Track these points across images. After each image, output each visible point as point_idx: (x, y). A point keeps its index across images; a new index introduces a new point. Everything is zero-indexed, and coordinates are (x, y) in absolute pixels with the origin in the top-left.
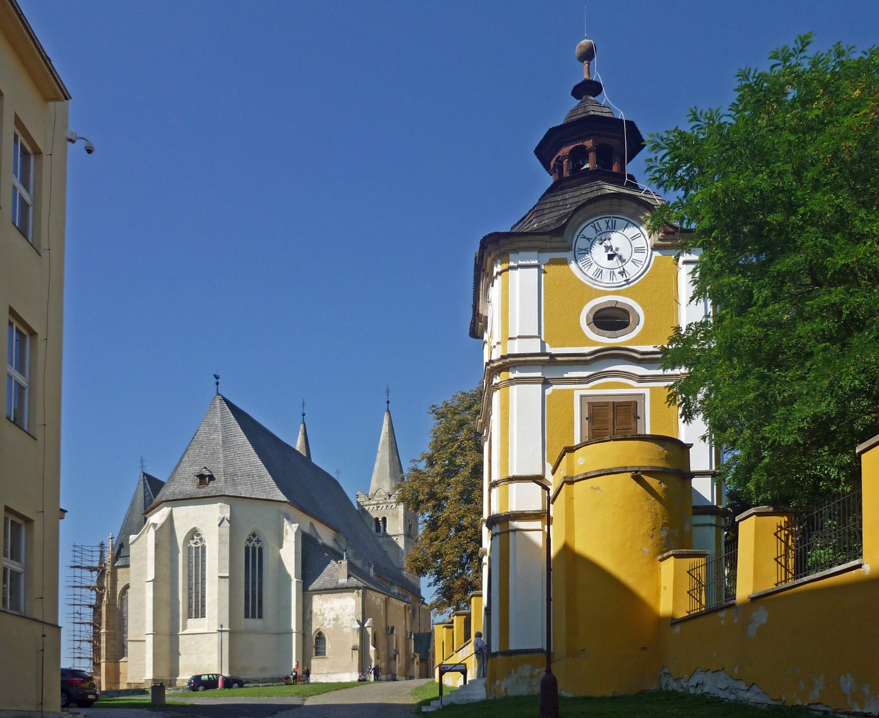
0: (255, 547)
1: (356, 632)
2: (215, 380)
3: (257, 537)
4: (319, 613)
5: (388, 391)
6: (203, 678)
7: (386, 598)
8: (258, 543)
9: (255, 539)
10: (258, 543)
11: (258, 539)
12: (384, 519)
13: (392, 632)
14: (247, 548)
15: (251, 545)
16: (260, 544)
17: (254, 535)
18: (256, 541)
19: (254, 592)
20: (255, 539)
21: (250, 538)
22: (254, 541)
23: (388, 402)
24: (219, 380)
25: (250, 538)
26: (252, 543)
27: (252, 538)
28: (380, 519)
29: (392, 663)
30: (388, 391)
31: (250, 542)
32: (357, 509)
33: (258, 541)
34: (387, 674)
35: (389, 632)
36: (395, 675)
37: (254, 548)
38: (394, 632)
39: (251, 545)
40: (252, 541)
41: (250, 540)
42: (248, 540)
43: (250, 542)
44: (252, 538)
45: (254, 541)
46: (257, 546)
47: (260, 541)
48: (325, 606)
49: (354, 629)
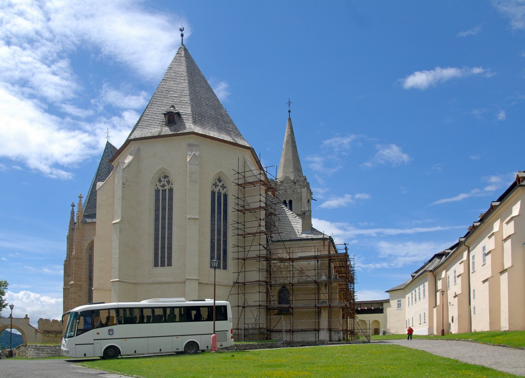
0: (221, 193)
3: (222, 183)
5: (289, 103)
8: (223, 189)
9: (220, 184)
10: (223, 189)
11: (223, 185)
14: (213, 193)
15: (216, 190)
16: (225, 190)
19: (219, 240)
20: (220, 184)
21: (216, 183)
23: (289, 111)
25: (216, 183)
26: (218, 188)
27: (218, 183)
30: (289, 103)
31: (216, 188)
33: (223, 187)
37: (219, 193)
39: (216, 190)
41: (215, 185)
42: (214, 185)
43: (216, 188)
44: (218, 183)
45: (219, 187)
46: (223, 192)
47: (225, 187)
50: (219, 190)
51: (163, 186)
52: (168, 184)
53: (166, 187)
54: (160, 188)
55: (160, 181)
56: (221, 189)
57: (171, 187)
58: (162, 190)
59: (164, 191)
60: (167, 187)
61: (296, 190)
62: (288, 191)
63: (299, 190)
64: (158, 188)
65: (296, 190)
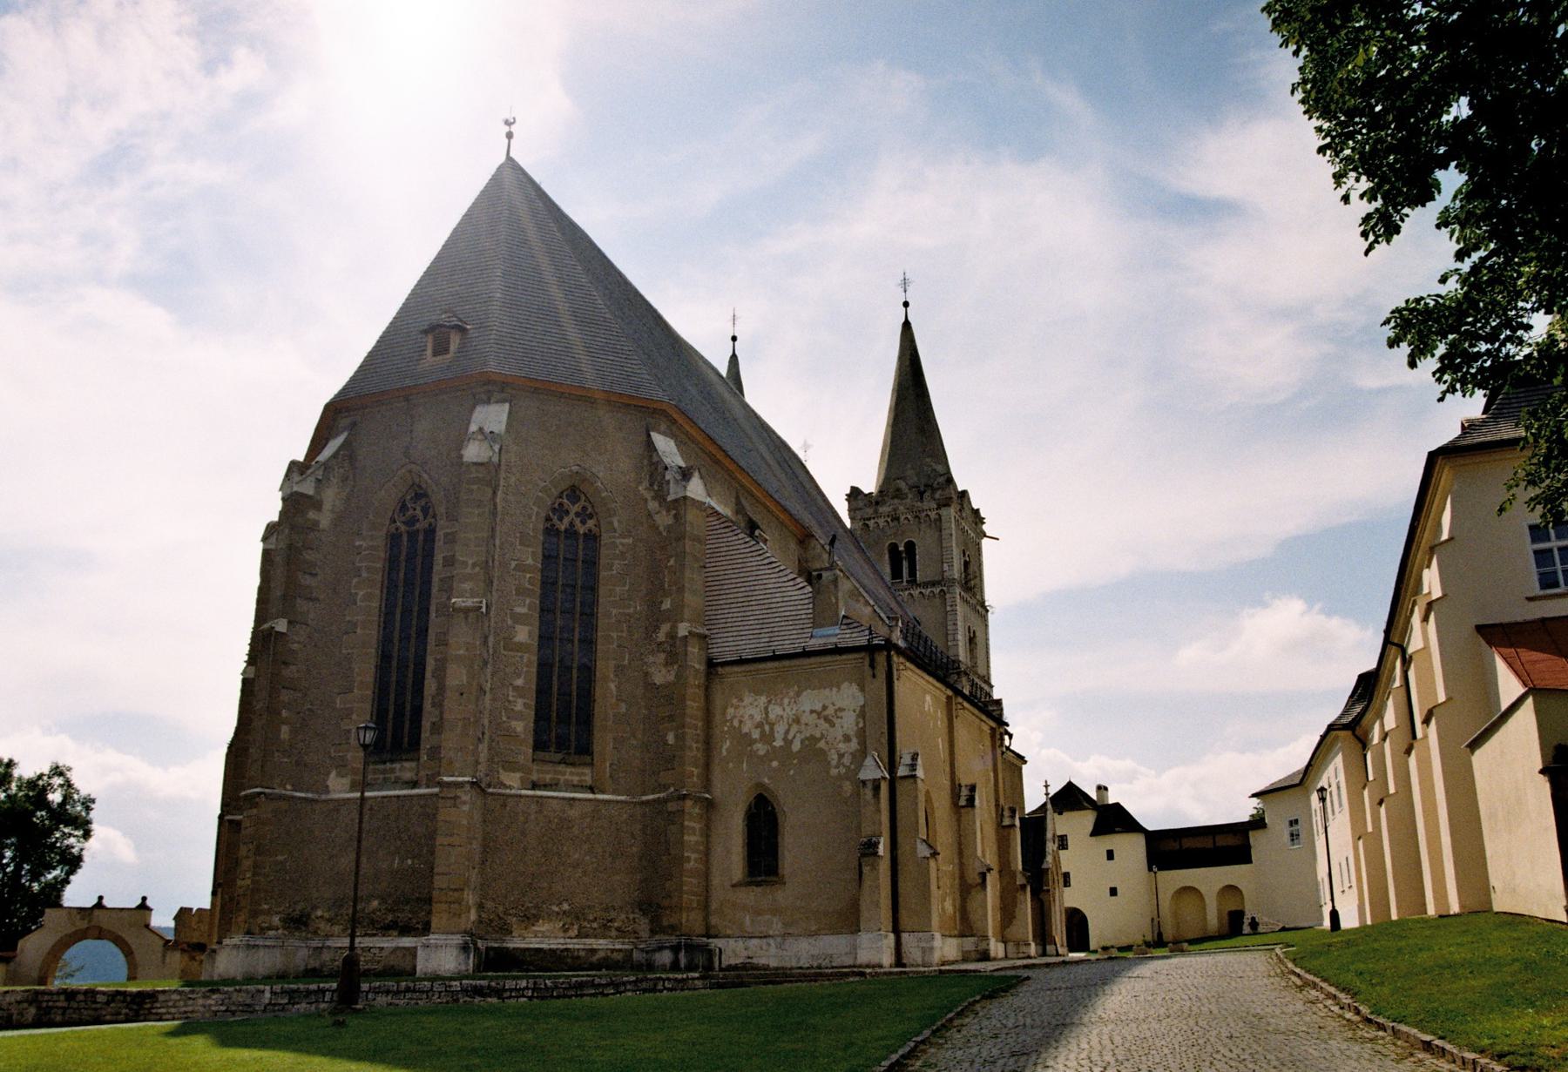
1: (868, 793)
2: (507, 129)
4: (756, 735)
6: (395, 933)
7: (949, 698)
8: (583, 522)
9: (576, 508)
10: (583, 522)
11: (584, 508)
12: (910, 546)
13: (971, 801)
16: (591, 523)
17: (574, 493)
18: (577, 514)
22: (572, 515)
24: (514, 128)
26: (566, 520)
28: (901, 548)
29: (976, 896)
32: (848, 523)
34: (962, 935)
35: (963, 802)
36: (986, 938)
38: (977, 802)
40: (567, 512)
41: (561, 511)
43: (561, 519)
48: (775, 711)
49: (864, 782)
50: (572, 524)
51: (412, 521)
52: (426, 515)
53: (418, 526)
54: (403, 528)
55: (403, 508)
56: (577, 522)
57: (430, 525)
58: (408, 532)
59: (412, 536)
60: (422, 525)
61: (924, 514)
62: (902, 518)
63: (933, 515)
64: (397, 529)
65: (924, 514)
